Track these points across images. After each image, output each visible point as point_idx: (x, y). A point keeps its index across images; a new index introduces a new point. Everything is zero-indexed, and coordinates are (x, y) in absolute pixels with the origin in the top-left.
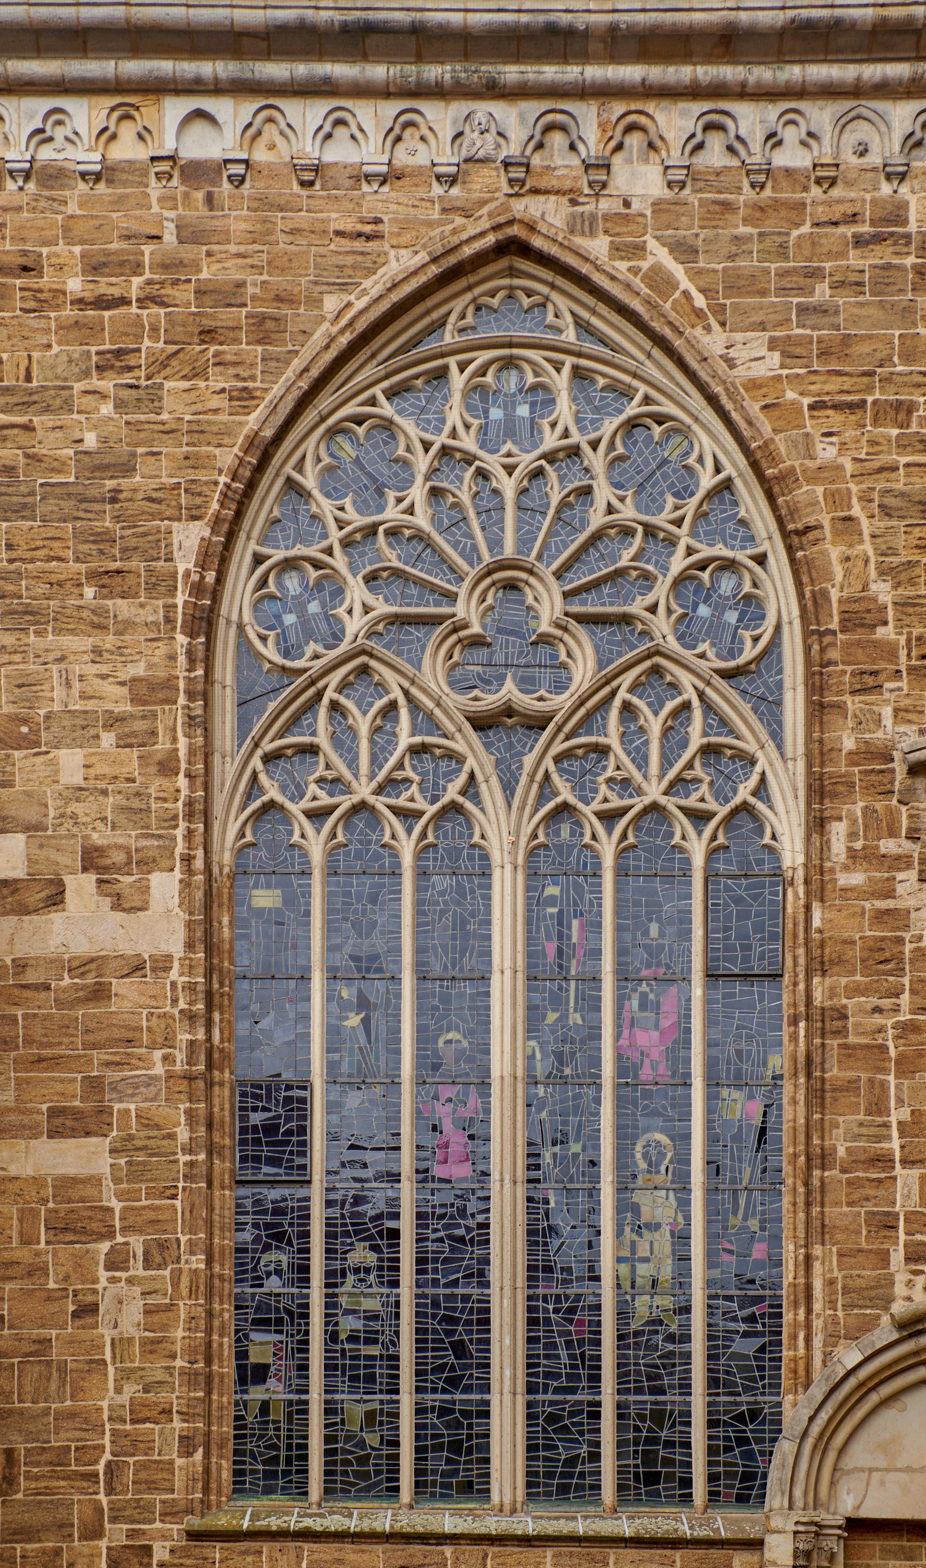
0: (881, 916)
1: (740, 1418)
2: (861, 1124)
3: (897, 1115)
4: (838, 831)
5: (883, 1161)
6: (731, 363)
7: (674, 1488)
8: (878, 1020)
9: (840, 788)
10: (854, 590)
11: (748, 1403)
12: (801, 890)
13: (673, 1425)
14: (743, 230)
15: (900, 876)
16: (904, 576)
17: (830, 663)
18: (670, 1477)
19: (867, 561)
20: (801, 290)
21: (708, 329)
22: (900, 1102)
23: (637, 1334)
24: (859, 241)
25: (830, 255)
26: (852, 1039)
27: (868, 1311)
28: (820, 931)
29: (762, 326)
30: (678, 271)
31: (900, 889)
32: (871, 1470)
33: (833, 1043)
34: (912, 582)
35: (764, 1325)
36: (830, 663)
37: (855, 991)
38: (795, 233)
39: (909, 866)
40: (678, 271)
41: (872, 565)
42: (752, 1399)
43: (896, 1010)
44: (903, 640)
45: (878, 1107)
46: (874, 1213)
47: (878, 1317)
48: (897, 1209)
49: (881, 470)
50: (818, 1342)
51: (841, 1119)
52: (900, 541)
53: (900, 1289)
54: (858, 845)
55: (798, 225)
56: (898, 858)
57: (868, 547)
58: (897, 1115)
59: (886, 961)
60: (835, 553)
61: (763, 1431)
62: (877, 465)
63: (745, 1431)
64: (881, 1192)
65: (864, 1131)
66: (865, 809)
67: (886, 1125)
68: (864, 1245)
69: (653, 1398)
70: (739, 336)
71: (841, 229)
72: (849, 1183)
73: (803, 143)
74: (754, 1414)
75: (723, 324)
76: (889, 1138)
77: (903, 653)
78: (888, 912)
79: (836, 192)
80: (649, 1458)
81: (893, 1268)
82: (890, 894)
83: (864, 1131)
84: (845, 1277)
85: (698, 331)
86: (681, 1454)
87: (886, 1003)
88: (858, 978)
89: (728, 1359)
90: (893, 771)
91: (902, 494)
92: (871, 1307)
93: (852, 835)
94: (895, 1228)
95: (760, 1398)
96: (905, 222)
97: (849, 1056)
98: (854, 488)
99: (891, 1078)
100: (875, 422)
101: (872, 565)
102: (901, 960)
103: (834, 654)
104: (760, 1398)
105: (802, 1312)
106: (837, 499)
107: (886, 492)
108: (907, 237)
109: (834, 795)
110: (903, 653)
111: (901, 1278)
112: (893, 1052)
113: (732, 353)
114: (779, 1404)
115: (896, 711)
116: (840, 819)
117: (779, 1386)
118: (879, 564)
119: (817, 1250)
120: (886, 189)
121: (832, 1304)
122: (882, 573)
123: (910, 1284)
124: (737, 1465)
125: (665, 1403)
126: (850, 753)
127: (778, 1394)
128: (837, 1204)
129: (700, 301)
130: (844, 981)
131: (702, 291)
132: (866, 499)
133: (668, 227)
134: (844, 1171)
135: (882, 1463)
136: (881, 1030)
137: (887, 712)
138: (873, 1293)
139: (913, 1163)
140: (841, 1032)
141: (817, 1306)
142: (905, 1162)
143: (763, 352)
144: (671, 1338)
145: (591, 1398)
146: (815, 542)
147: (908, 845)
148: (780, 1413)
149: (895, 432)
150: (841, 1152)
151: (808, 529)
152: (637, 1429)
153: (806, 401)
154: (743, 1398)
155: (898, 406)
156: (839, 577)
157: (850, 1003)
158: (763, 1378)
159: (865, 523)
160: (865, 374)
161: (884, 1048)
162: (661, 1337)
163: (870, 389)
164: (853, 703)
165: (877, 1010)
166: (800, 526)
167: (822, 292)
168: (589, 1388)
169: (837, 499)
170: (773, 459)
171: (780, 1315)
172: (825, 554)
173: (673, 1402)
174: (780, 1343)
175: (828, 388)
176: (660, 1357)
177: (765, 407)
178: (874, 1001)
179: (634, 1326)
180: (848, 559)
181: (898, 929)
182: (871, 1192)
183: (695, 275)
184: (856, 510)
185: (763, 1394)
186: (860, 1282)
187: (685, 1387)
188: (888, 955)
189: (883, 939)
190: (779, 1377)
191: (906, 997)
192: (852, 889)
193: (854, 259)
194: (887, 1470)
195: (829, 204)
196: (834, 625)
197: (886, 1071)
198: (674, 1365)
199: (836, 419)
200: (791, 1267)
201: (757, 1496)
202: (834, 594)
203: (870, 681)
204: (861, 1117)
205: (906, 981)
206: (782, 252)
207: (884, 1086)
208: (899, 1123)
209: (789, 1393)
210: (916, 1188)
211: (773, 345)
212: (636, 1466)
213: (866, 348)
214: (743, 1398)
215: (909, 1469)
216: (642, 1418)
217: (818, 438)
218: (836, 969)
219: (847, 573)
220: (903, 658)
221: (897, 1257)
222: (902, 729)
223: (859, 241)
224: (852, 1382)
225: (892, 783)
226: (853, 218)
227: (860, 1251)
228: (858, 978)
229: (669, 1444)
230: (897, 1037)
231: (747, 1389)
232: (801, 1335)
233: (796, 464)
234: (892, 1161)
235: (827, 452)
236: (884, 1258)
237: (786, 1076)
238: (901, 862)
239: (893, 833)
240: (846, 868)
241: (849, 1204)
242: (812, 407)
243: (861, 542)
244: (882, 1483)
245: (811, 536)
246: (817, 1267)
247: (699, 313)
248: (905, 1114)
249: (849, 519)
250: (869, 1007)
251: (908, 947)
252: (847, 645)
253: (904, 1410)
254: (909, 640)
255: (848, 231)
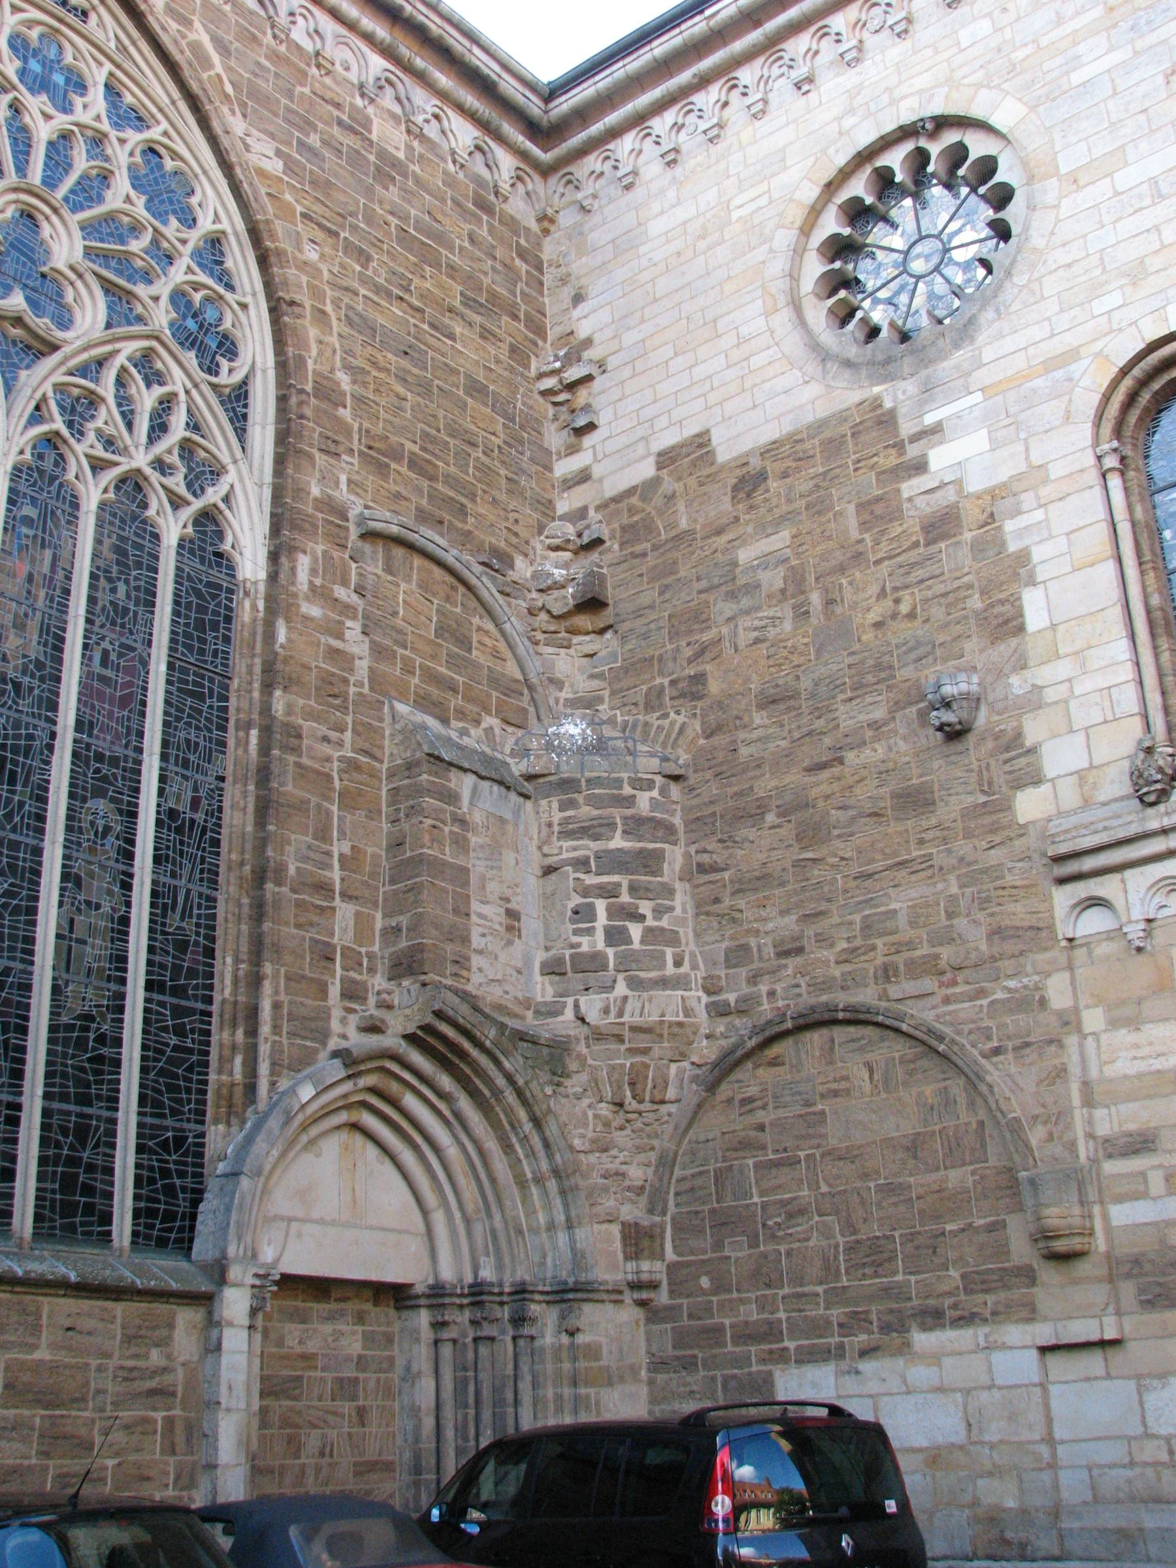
0: (334, 654)
1: (164, 1145)
2: (309, 847)
3: (339, 847)
4: (304, 563)
5: (324, 888)
6: (247, 148)
7: (92, 1224)
8: (327, 749)
9: (307, 526)
10: (324, 368)
11: (174, 1129)
12: (261, 605)
13: (97, 1146)
14: (263, 61)
15: (349, 623)
16: (359, 377)
17: (302, 417)
18: (89, 1209)
19: (334, 351)
20: (301, 129)
21: (233, 112)
22: (342, 834)
23: (70, 1028)
24: (340, 123)
25: (320, 119)
26: (305, 761)
27: (308, 1043)
28: (282, 646)
29: (272, 136)
30: (216, 58)
31: (348, 634)
32: (290, 1220)
33: (292, 759)
34: (365, 384)
35: (193, 1041)
36: (302, 417)
37: (310, 715)
38: (299, 89)
39: (354, 618)
40: (216, 58)
41: (338, 358)
42: (178, 1125)
43: (340, 744)
44: (356, 426)
45: (323, 834)
46: (317, 941)
47: (315, 1051)
48: (335, 940)
49: (347, 289)
50: (264, 1068)
51: (293, 837)
52: (358, 350)
53: (335, 1025)
54: (318, 582)
55: (302, 85)
56: (347, 606)
57: (334, 340)
58: (339, 847)
59: (335, 696)
60: (313, 333)
61: (185, 1164)
62: (345, 284)
63: (167, 1162)
64: (323, 921)
65: (312, 855)
66: (325, 552)
67: (329, 854)
68: (307, 972)
69: (78, 1109)
70: (254, 132)
71: (330, 108)
72: (299, 904)
73: (309, 34)
74: (180, 1141)
75: (245, 116)
76: (329, 867)
77: (356, 437)
78: (338, 651)
79: (328, 81)
80: (68, 1183)
81: (331, 1002)
82: (340, 636)
83: (312, 855)
84: (290, 1003)
85: (225, 109)
86: (103, 1182)
87: (333, 735)
88: (312, 703)
89: (159, 1074)
90: (347, 529)
91: (361, 316)
92: (312, 1040)
93: (313, 571)
94: (332, 960)
95: (186, 1125)
96: (370, 132)
97: (302, 776)
98: (329, 293)
99: (335, 808)
100: (345, 253)
101: (338, 358)
102: (346, 700)
103: (308, 412)
104: (186, 1125)
105: (240, 1035)
106: (316, 293)
107: (349, 307)
108: (371, 142)
109: (302, 530)
110: (356, 437)
111: (336, 1014)
112: (337, 784)
113: (249, 140)
114: (202, 1135)
115: (349, 481)
116: (305, 552)
117: (204, 1113)
118: (343, 359)
119: (268, 968)
120: (359, 102)
121: (276, 1029)
122: (347, 367)
123: (343, 1021)
124: (158, 1201)
125: (90, 1117)
126: (316, 499)
127: (203, 1122)
128: (287, 923)
129: (229, 89)
130: (301, 702)
131: (232, 83)
132: (336, 303)
133: (212, 22)
134: (294, 890)
135: (300, 1213)
136: (328, 759)
137: (343, 478)
138: (313, 1025)
139: (350, 898)
140: (297, 750)
141: (265, 1029)
142: (345, 896)
143: (271, 154)
144: (101, 1039)
145: (11, 1098)
146: (299, 316)
147: (355, 598)
148: (203, 1145)
149: (358, 268)
150: (292, 870)
151: (292, 303)
152: (58, 1145)
153: (299, 209)
154: (169, 1122)
155: (361, 251)
156: (314, 353)
157: (307, 725)
158: (189, 1101)
159: (335, 322)
160: (340, 214)
161: (329, 778)
162: (92, 1036)
163: (343, 227)
164: (320, 459)
165: (326, 739)
166: (287, 297)
167: (314, 140)
168: (11, 1085)
169: (316, 293)
170: (273, 237)
171: (208, 1033)
172: (305, 328)
173: (99, 1118)
174: (206, 1064)
175: (314, 208)
176: (90, 1060)
177: (269, 194)
178: (323, 730)
179: (65, 1019)
180: (321, 342)
181: (343, 670)
182: (315, 919)
183: (228, 69)
184: (329, 308)
185: (189, 1120)
186: (303, 1011)
187: (113, 1101)
188: (336, 691)
189: (333, 675)
190: (204, 1102)
191: (348, 736)
192: (312, 619)
193: (336, 131)
194: (304, 1221)
195: (324, 85)
196: (309, 388)
197: (331, 800)
198: (101, 1072)
199: (320, 235)
200: (228, 981)
201: (176, 1241)
202: (310, 362)
203: (333, 448)
204: (309, 839)
205: (349, 719)
206: (290, 94)
207: (328, 813)
208: (341, 855)
209: (216, 1121)
210: (352, 923)
211: (279, 153)
212: (53, 1191)
213: (342, 198)
214: (169, 1122)
215: (321, 1222)
216: (65, 1131)
217: (305, 241)
218: (295, 688)
219: (320, 353)
220: (356, 442)
221: (335, 991)
222: (352, 498)
223: (340, 123)
224: (300, 1117)
225: (346, 538)
226: (338, 106)
227: (303, 977)
228: (312, 703)
229: (91, 1168)
230: (340, 771)
231: (174, 1112)
232: (238, 1060)
233: (289, 250)
234: (333, 891)
235: (312, 255)
236: (322, 991)
237: (229, 779)
238: (347, 610)
239: (345, 583)
240: (307, 599)
241: (298, 926)
242: (304, 215)
243: (331, 334)
244: (299, 1235)
245: (297, 310)
246: (267, 987)
247: (227, 96)
248: (346, 848)
249: (323, 312)
250: (320, 734)
251: (352, 690)
252: (317, 410)
253: (318, 1155)
254: (360, 429)
255: (336, 113)
